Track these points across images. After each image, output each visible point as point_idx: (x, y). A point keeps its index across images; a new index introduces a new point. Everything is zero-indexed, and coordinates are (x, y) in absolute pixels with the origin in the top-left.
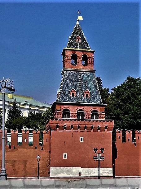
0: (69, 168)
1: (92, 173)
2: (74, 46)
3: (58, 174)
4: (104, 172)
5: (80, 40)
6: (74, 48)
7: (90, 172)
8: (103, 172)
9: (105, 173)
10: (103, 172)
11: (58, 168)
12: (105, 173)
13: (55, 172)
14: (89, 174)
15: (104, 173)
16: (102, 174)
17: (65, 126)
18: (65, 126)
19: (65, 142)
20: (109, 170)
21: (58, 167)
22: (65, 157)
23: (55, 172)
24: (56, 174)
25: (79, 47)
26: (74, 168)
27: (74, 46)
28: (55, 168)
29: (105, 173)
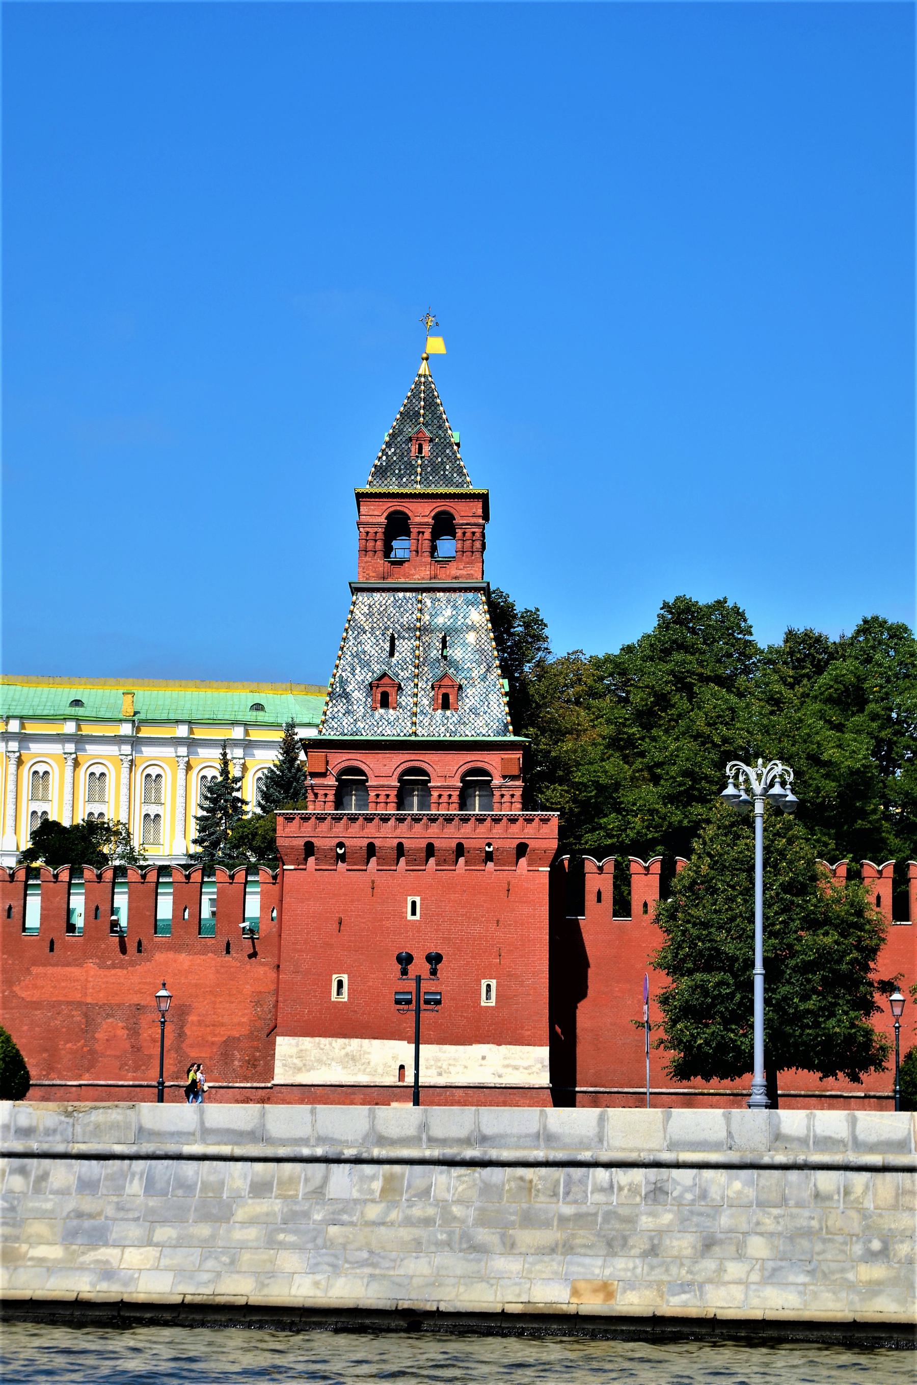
0: (355, 1042)
1: (452, 1069)
3: (309, 1071)
4: (507, 1066)
5: (426, 448)
6: (400, 485)
7: (445, 1067)
8: (507, 1066)
9: (516, 1068)
12: (516, 1072)
14: (440, 1074)
15: (510, 1069)
16: (500, 1076)
17: (341, 845)
18: (341, 845)
19: (340, 923)
21: (308, 1039)
23: (296, 1061)
24: (299, 1069)
27: (401, 477)
28: (297, 1045)
29: (516, 1068)
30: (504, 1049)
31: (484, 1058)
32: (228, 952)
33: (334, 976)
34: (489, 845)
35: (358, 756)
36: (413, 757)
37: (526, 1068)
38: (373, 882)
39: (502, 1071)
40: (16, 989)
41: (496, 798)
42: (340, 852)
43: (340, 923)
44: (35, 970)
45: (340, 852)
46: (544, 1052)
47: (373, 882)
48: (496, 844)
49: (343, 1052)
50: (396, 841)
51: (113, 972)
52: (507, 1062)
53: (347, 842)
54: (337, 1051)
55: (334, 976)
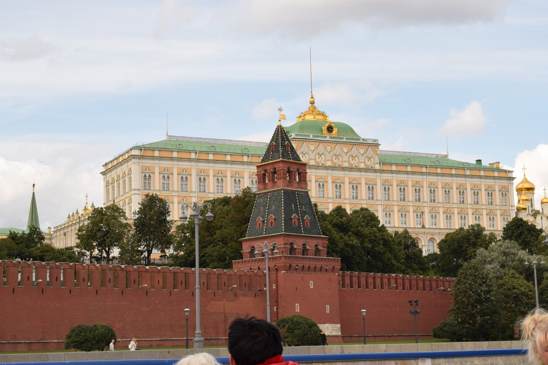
2: (287, 157)
8: (332, 330)
9: (334, 330)
10: (332, 330)
15: (333, 331)
16: (331, 333)
17: (297, 266)
19: (296, 288)
27: (287, 157)
29: (334, 330)
30: (331, 325)
31: (328, 327)
33: (296, 304)
35: (294, 239)
36: (305, 240)
37: (336, 330)
38: (302, 277)
39: (332, 331)
40: (207, 308)
41: (322, 253)
42: (297, 267)
43: (296, 288)
44: (212, 302)
46: (339, 326)
47: (302, 277)
48: (329, 266)
50: (308, 265)
51: (230, 303)
53: (299, 265)
55: (296, 304)
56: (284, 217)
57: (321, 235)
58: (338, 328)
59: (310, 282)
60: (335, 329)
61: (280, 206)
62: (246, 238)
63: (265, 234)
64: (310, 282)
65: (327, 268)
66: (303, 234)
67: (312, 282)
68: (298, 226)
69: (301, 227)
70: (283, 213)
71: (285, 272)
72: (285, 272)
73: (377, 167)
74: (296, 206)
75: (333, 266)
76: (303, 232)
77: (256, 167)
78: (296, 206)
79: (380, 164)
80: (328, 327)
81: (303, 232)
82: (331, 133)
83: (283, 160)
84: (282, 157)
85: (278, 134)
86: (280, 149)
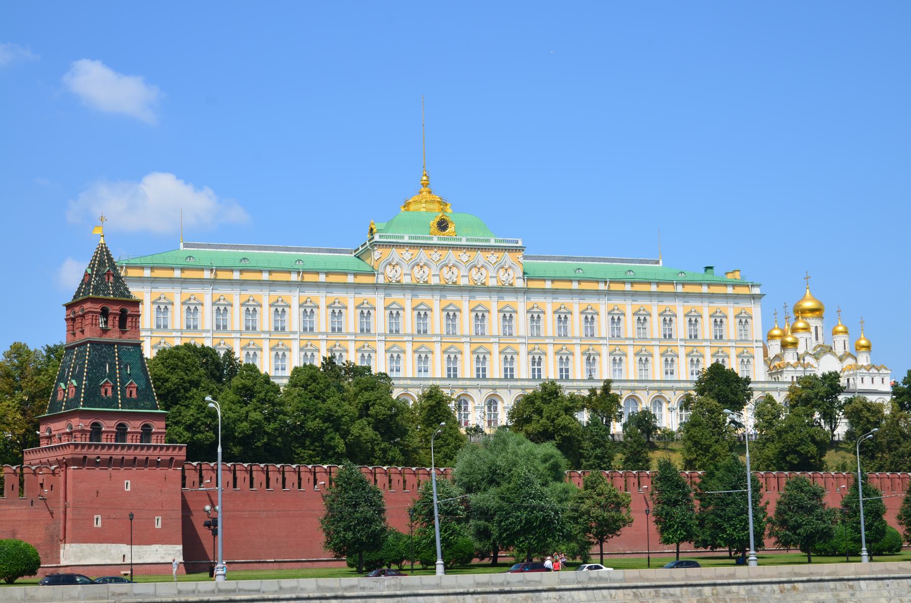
0: (105, 545)
2: (104, 291)
8: (166, 554)
9: (170, 554)
10: (166, 554)
11: (84, 546)
13: (80, 554)
14: (140, 558)
15: (167, 556)
16: (163, 558)
17: (98, 458)
18: (98, 458)
19: (97, 493)
20: (177, 549)
21: (85, 544)
22: (97, 524)
23: (80, 554)
25: (111, 292)
26: (114, 545)
27: (104, 291)
30: (164, 546)
31: (157, 550)
32: (32, 505)
34: (159, 458)
38: (110, 474)
43: (97, 493)
45: (98, 460)
46: (180, 547)
47: (110, 474)
49: (100, 550)
52: (166, 552)
54: (97, 549)
56: (85, 384)
57: (157, 409)
58: (179, 551)
59: (126, 482)
60: (171, 552)
61: (82, 368)
62: (46, 415)
63: (64, 410)
64: (126, 482)
65: (159, 460)
66: (120, 410)
67: (129, 482)
68: (113, 396)
69: (118, 398)
70: (84, 378)
71: (76, 467)
72: (76, 467)
73: (519, 284)
74: (112, 367)
75: (170, 457)
76: (120, 405)
77: (65, 308)
78: (112, 367)
79: (524, 280)
80: (157, 550)
81: (120, 405)
82: (444, 231)
83: (94, 296)
84: (92, 293)
85: (96, 257)
86: (93, 279)
